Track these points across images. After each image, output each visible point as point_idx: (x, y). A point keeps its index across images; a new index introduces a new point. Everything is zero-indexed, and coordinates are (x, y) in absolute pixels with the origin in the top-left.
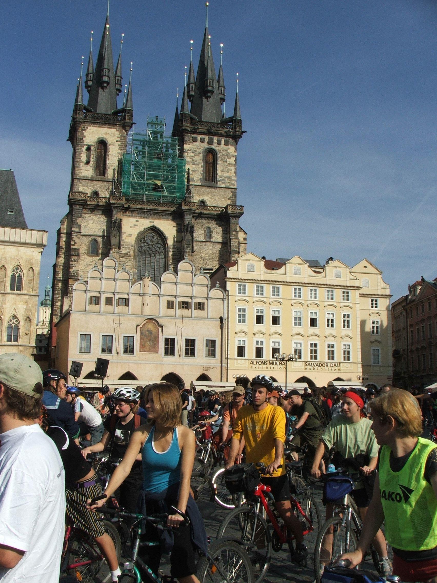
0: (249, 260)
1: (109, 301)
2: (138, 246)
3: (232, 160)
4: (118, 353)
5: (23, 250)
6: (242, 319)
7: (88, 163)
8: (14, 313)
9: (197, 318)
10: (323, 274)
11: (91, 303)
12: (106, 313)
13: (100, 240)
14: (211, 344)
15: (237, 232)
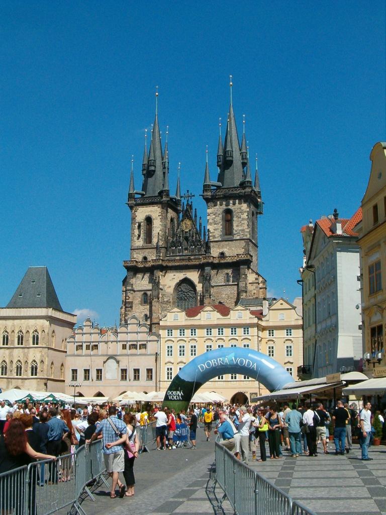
0: (175, 312)
1: (88, 347)
2: (176, 293)
3: (245, 216)
4: (92, 380)
5: (38, 321)
6: (170, 353)
7: (139, 236)
8: (33, 359)
9: (140, 355)
10: (229, 317)
11: (77, 350)
12: (86, 355)
13: (149, 293)
14: (149, 371)
15: (246, 275)
